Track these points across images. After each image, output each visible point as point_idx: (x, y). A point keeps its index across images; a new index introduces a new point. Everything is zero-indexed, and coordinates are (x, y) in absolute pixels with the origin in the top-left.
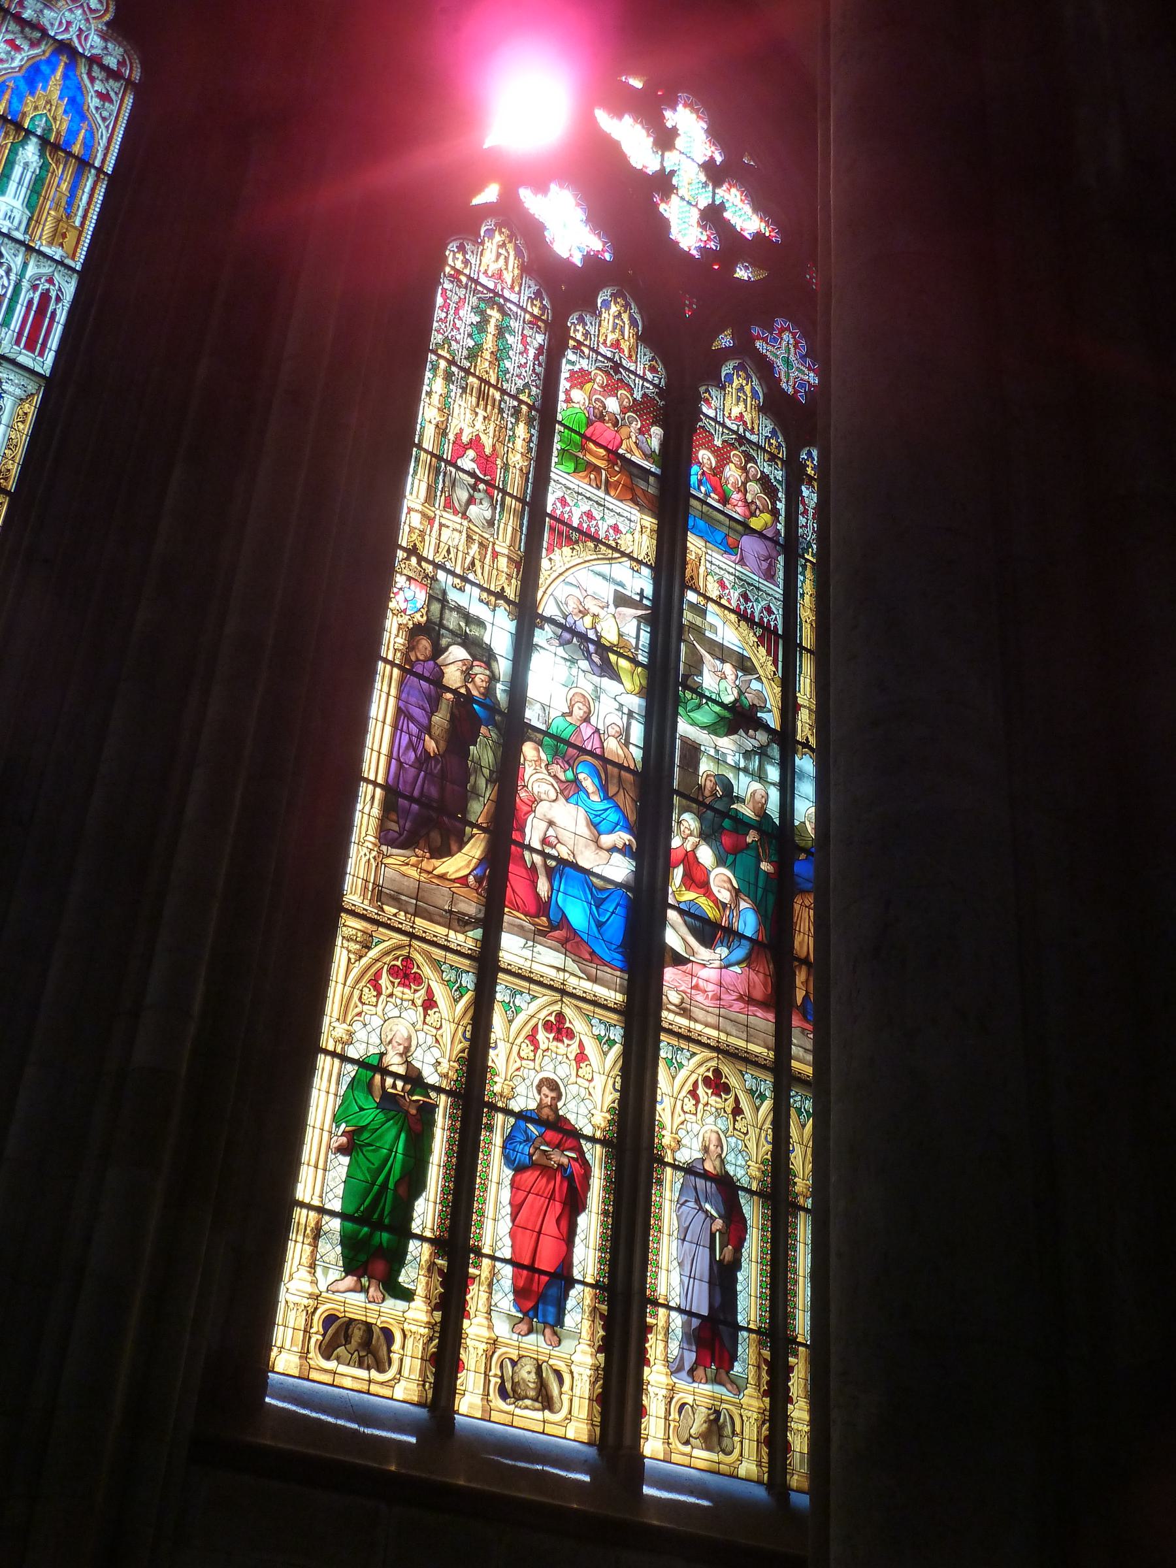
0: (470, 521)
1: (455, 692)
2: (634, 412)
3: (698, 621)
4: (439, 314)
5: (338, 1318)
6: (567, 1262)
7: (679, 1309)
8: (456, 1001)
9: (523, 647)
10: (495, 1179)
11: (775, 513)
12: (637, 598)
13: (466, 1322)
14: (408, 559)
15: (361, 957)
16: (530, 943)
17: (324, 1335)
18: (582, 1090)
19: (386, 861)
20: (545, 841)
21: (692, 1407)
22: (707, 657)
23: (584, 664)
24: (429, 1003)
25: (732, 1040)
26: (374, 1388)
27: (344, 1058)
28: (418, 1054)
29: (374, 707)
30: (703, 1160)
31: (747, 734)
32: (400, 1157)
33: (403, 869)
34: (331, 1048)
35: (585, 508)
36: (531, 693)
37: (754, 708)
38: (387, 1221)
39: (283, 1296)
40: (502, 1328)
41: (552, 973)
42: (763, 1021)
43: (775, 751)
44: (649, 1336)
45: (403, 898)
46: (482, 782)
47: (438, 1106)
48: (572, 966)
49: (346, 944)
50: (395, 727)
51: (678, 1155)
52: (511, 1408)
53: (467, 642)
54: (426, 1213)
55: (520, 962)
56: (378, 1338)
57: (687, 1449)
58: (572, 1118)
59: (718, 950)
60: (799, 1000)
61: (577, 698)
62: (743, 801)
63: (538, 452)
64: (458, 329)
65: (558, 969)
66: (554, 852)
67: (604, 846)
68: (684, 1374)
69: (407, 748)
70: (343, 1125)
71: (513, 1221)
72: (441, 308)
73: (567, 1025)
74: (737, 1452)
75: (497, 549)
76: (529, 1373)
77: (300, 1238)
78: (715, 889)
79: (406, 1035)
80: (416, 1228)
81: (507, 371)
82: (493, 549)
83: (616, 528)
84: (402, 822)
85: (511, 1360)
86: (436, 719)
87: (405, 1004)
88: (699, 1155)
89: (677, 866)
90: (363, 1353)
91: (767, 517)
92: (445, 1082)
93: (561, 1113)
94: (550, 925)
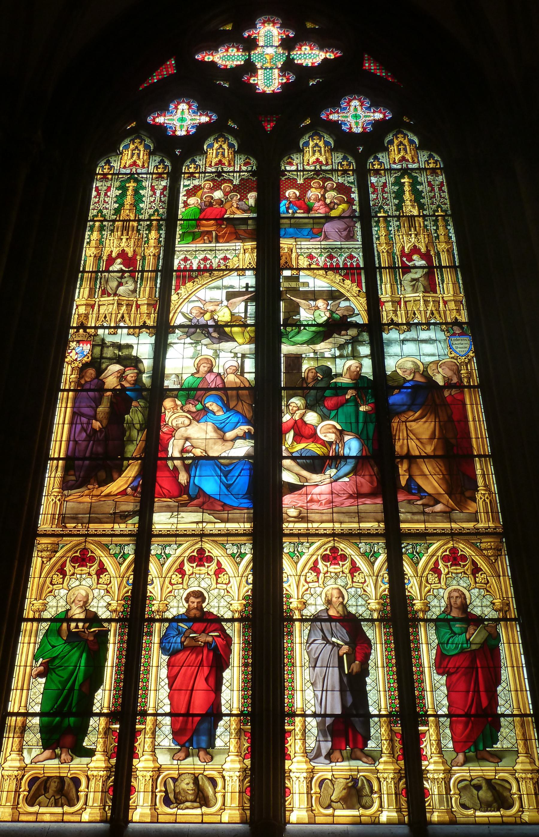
1: (113, 390)
3: (293, 284)
4: (94, 200)
5: (39, 778)
6: (217, 703)
7: (314, 715)
8: (121, 564)
10: (155, 664)
12: (244, 290)
13: (135, 761)
14: (78, 331)
15: (51, 559)
17: (29, 792)
18: (222, 591)
19: (66, 499)
20: (183, 450)
21: (331, 780)
22: (302, 302)
23: (206, 341)
24: (102, 570)
30: (327, 610)
31: (339, 334)
32: (82, 668)
33: (80, 499)
34: (31, 616)
35: (202, 256)
36: (167, 372)
37: (344, 317)
38: (74, 710)
40: (164, 759)
41: (194, 526)
42: (374, 506)
43: (365, 336)
44: (289, 739)
45: (80, 516)
46: (135, 433)
47: (110, 631)
48: (208, 517)
49: (40, 554)
50: (71, 423)
51: (305, 612)
53: (118, 360)
54: (103, 698)
55: (169, 526)
56: (69, 785)
57: (330, 811)
58: (214, 611)
59: (328, 472)
60: (403, 483)
62: (341, 375)
63: (165, 241)
65: (197, 523)
67: (229, 439)
68: (322, 759)
69: (80, 432)
70: (41, 659)
71: (170, 687)
72: (95, 197)
73: (207, 554)
75: (139, 303)
76: (188, 784)
77: (11, 735)
78: (322, 436)
79: (84, 594)
80: (96, 709)
81: (142, 209)
83: (225, 259)
84: (77, 474)
85: (173, 778)
86: (100, 409)
87: (84, 576)
88: (323, 608)
89: (288, 431)
90: (57, 797)
92: (115, 615)
93: (205, 610)
94: (191, 498)
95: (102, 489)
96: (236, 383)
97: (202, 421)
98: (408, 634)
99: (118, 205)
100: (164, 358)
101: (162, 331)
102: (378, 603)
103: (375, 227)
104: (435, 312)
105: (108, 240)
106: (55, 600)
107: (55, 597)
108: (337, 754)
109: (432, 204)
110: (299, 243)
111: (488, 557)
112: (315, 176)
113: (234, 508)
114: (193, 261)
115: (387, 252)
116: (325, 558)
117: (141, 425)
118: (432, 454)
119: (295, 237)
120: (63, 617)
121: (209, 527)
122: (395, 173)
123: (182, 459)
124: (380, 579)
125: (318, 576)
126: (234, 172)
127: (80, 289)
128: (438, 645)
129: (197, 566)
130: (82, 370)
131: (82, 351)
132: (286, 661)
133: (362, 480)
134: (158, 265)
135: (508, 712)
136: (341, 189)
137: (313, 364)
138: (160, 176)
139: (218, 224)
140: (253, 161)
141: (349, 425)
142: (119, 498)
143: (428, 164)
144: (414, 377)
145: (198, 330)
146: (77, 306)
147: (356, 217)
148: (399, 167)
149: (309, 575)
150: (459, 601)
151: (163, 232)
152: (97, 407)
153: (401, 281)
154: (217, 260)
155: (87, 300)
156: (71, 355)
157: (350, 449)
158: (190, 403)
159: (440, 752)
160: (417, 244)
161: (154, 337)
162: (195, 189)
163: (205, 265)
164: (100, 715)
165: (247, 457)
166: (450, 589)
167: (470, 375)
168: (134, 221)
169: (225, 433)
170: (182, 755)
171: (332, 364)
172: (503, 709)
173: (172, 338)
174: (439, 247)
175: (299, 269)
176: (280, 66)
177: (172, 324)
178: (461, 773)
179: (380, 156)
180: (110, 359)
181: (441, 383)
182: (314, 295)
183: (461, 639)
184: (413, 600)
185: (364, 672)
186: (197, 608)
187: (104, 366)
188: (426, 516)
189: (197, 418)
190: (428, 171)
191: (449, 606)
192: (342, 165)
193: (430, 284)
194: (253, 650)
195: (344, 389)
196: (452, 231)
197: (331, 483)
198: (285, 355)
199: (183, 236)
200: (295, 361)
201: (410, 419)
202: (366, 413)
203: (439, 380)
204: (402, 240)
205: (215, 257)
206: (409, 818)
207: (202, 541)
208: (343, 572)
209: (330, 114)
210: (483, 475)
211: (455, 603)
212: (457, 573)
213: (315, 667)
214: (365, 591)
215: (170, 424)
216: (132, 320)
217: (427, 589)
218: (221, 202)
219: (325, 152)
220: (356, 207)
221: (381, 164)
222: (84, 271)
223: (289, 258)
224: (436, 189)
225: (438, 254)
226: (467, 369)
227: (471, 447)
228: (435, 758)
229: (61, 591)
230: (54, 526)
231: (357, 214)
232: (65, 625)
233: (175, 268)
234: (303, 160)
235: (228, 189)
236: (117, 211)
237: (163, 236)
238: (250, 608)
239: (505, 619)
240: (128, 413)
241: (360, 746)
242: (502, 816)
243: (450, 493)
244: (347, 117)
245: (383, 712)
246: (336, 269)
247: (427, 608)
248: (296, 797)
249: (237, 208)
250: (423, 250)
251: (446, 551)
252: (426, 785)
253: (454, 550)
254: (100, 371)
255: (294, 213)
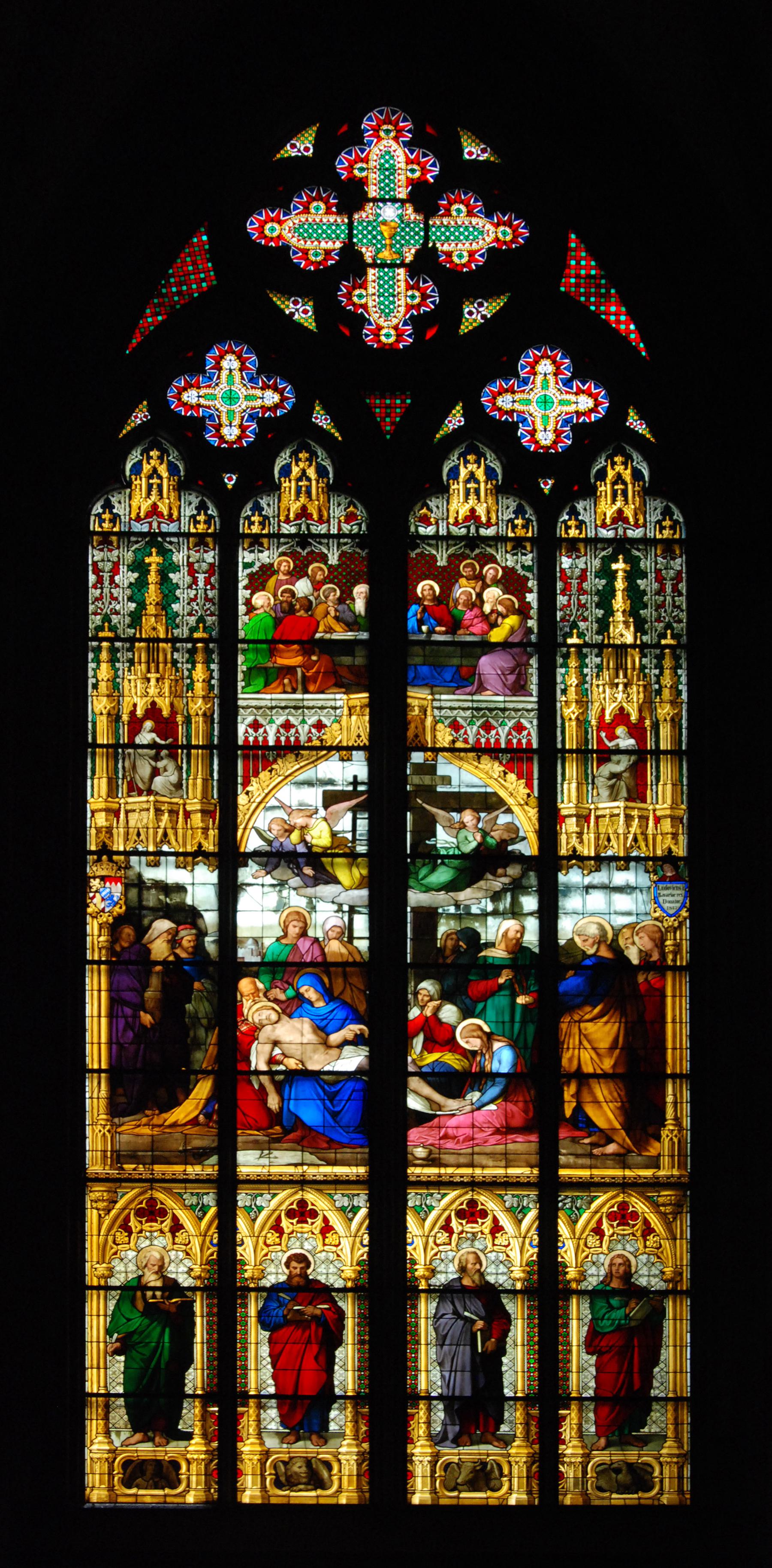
0: (157, 794)
1: (164, 963)
2: (331, 582)
3: (427, 780)
4: (94, 593)
8: (201, 1219)
9: (228, 893)
10: (253, 1341)
11: (523, 611)
12: (350, 788)
13: (240, 1445)
14: (99, 860)
15: (109, 1211)
16: (266, 1152)
19: (119, 1130)
20: (272, 1061)
22: (441, 813)
23: (295, 881)
24: (177, 1227)
25: (487, 1171)
26: (169, 1500)
27: (107, 1288)
28: (172, 1268)
29: (88, 1007)
31: (494, 874)
32: (167, 1345)
33: (137, 1130)
34: (95, 1283)
35: (280, 720)
36: (241, 933)
37: (503, 843)
39: (88, 1455)
40: (271, 1443)
41: (291, 1170)
42: (524, 1145)
43: (532, 879)
46: (201, 1033)
48: (309, 1157)
49: (94, 1205)
50: (111, 1016)
51: (433, 1281)
52: (287, 1492)
53: (167, 912)
54: (195, 1378)
55: (259, 1170)
57: (455, 1494)
58: (322, 1279)
59: (468, 1097)
60: (568, 1112)
61: (290, 918)
62: (493, 945)
63: (221, 687)
64: (116, 599)
65: (296, 1165)
66: (282, 1068)
68: (448, 1443)
69: (125, 1030)
71: (274, 1367)
73: (310, 1207)
74: (505, 1488)
75: (188, 808)
77: (94, 1417)
78: (462, 1043)
79: (158, 1256)
80: (189, 1390)
81: (177, 615)
82: (185, 809)
83: (319, 726)
85: (283, 1462)
86: (148, 994)
87: (155, 1234)
88: (455, 1276)
89: (416, 1035)
91: (512, 620)
94: (286, 1131)
95: (165, 1115)
96: (342, 955)
97: (296, 1014)
98: (557, 1308)
99: (134, 605)
100: (235, 911)
101: (228, 860)
102: (524, 1271)
103: (561, 667)
104: (640, 837)
105: (126, 683)
106: (122, 1265)
107: (122, 1260)
108: (465, 1438)
109: (658, 620)
110: (437, 697)
111: (665, 1214)
112: (467, 551)
113: (342, 1145)
114: (268, 727)
115: (577, 719)
116: (460, 1214)
117: (209, 1020)
118: (611, 1071)
119: (431, 686)
120: (135, 1284)
121: (311, 1172)
122: (604, 549)
123: (270, 1073)
124: (527, 1241)
125: (450, 1237)
126: (328, 536)
127: (92, 779)
128: (591, 1320)
129: (298, 1222)
130: (114, 928)
131: (111, 897)
132: (409, 1338)
133: (515, 1108)
134: (212, 735)
135: (662, 1395)
136: (511, 582)
137: (453, 925)
138: (201, 540)
139: (306, 653)
140: (360, 512)
141: (501, 1025)
142: (189, 1130)
143: (662, 528)
144: (598, 950)
145: (282, 862)
146: (93, 812)
147: (530, 644)
148: (610, 534)
149: (439, 1235)
150: (622, 1269)
151: (214, 666)
152: (144, 991)
153: (594, 777)
154: (306, 727)
155: (106, 801)
156: (95, 901)
157: (500, 1062)
158: (276, 987)
159: (581, 1435)
160: (625, 705)
161: (216, 873)
162: (264, 573)
163: (288, 738)
164: (194, 1396)
165: (359, 1071)
166: (613, 1254)
167: (678, 946)
168: (166, 641)
169: (328, 1035)
170: (292, 1438)
171: (481, 925)
172: (657, 1392)
173: (245, 874)
174: (659, 711)
175: (436, 750)
176: (409, 258)
177: (242, 850)
178: (600, 1457)
179: (580, 506)
180: (152, 909)
181: (635, 961)
182: (459, 801)
183: (621, 1313)
184: (567, 1267)
185: (501, 1351)
186: (300, 1275)
187: (146, 922)
188: (594, 1160)
189: (288, 1011)
190: (659, 547)
191: (609, 1276)
192: (514, 527)
193: (637, 785)
194: (370, 1324)
195: (496, 969)
196: (684, 679)
197: (472, 1111)
198: (413, 909)
199: (249, 674)
200: (428, 917)
201: (587, 1017)
202: (525, 1006)
203: (633, 955)
204: (602, 696)
205: (303, 722)
206: (540, 1501)
207: (303, 1190)
208: (482, 1233)
209: (500, 393)
210: (675, 1103)
211: (617, 1272)
212: (624, 1235)
213: (442, 1345)
214: (508, 1256)
215: (250, 1019)
216: (180, 839)
217: (584, 1254)
218: (308, 605)
219: (486, 495)
220: (532, 623)
221: (580, 525)
222: (95, 745)
223: (420, 728)
224: (669, 589)
225: (656, 726)
226: (675, 939)
227: (664, 1062)
228: (575, 1442)
229: (129, 1252)
230: (107, 1167)
231: (533, 638)
232: (139, 1293)
233: (240, 742)
234: (448, 510)
235: (319, 577)
236: (136, 619)
237: (216, 674)
238: (366, 1276)
239: (674, 1293)
240: (190, 1002)
241: (491, 1429)
242: (639, 1498)
243: (628, 1127)
244: (528, 402)
245: (519, 1395)
246: (493, 752)
247: (582, 1276)
248: (419, 1481)
249: (336, 618)
250: (634, 718)
251: (613, 1207)
252: (562, 1468)
253: (623, 1206)
254: (142, 930)
255: (431, 632)
